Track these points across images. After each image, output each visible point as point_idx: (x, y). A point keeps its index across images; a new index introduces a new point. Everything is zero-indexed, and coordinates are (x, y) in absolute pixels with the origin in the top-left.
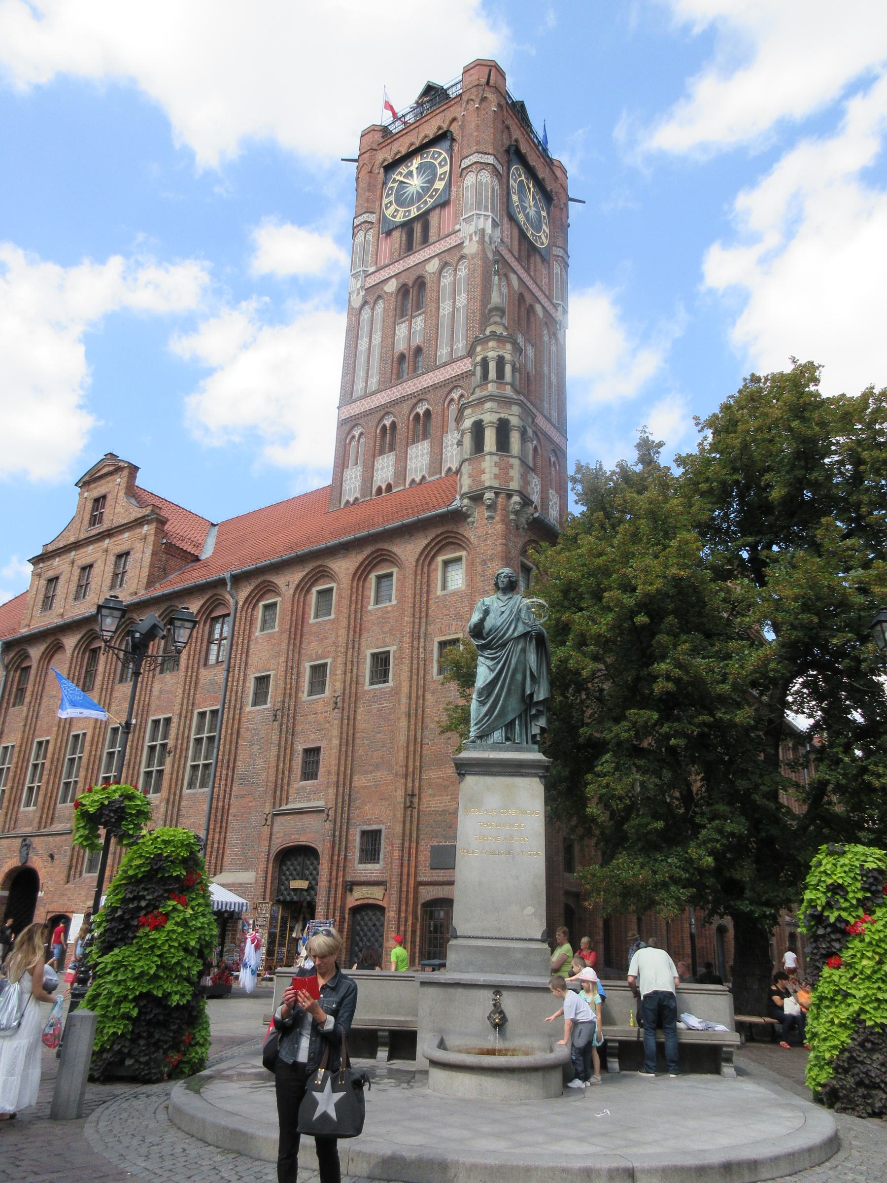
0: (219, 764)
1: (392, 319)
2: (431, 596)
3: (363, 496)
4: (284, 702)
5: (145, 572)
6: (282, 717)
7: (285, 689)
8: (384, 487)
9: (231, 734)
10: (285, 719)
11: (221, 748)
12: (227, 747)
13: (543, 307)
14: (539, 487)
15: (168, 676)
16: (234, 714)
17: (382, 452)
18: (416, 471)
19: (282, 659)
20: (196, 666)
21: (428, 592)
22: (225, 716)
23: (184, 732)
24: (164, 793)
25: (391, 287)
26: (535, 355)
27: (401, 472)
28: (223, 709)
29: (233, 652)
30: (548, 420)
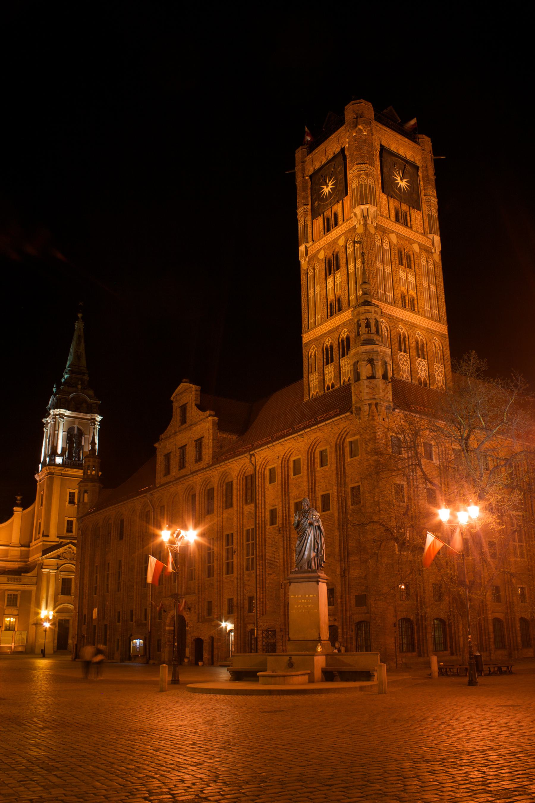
0: (258, 558)
1: (324, 277)
2: (346, 461)
3: (320, 391)
4: (283, 523)
5: (211, 451)
6: (283, 531)
7: (283, 516)
8: (330, 385)
9: (262, 541)
10: (285, 532)
11: (258, 549)
12: (261, 548)
13: (419, 244)
14: (426, 366)
15: (230, 510)
16: (262, 530)
17: (327, 364)
18: (345, 375)
19: (280, 500)
20: (241, 504)
21: (344, 459)
22: (257, 533)
23: (240, 541)
24: (235, 574)
25: (321, 256)
26: (416, 279)
27: (339, 375)
28: (256, 528)
29: (257, 497)
30: (431, 318)
